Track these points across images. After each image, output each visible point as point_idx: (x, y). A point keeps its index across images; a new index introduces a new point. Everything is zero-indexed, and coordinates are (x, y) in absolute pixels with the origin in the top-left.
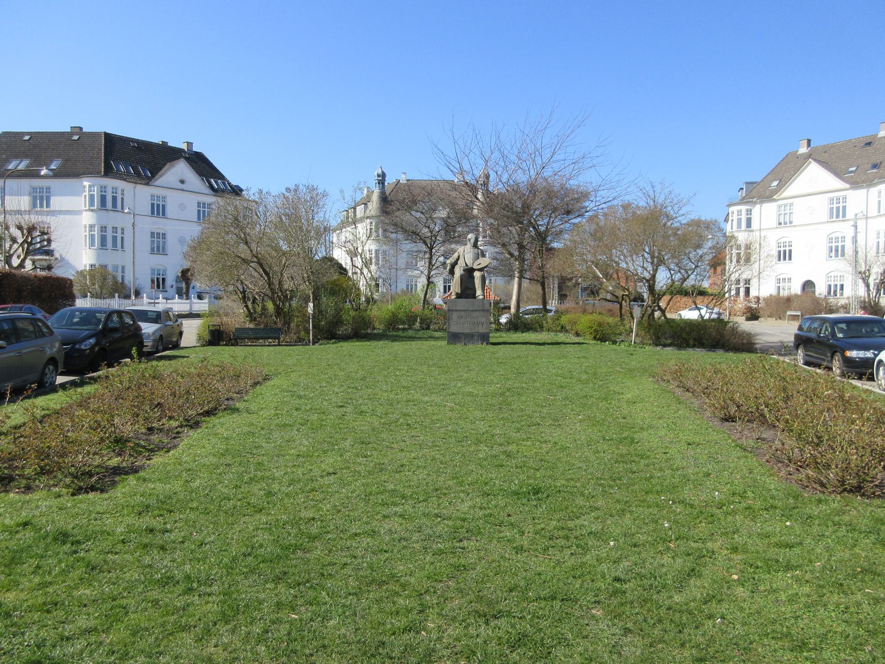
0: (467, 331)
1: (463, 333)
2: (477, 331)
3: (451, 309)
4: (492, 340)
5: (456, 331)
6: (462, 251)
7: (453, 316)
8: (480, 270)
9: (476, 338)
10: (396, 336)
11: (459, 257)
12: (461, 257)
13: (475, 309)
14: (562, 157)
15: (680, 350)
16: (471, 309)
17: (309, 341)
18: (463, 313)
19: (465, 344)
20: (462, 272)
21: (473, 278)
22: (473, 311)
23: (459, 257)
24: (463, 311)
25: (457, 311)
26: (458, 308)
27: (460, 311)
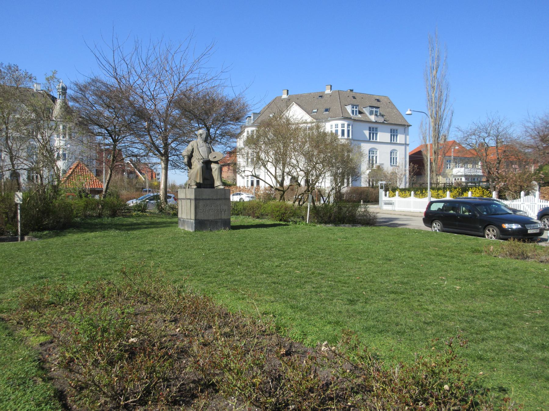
0: (211, 218)
1: (208, 220)
2: (220, 218)
3: (198, 198)
4: (233, 224)
5: (203, 219)
6: (195, 145)
7: (200, 204)
8: (216, 162)
9: (219, 224)
10: (132, 224)
11: (193, 149)
12: (195, 149)
13: (219, 197)
14: (196, 76)
15: (336, 226)
16: (215, 198)
17: (16, 233)
18: (208, 202)
19: (210, 230)
20: (202, 165)
21: (211, 170)
22: (216, 199)
23: (193, 149)
24: (209, 199)
25: (203, 199)
26: (204, 197)
27: (206, 199)
